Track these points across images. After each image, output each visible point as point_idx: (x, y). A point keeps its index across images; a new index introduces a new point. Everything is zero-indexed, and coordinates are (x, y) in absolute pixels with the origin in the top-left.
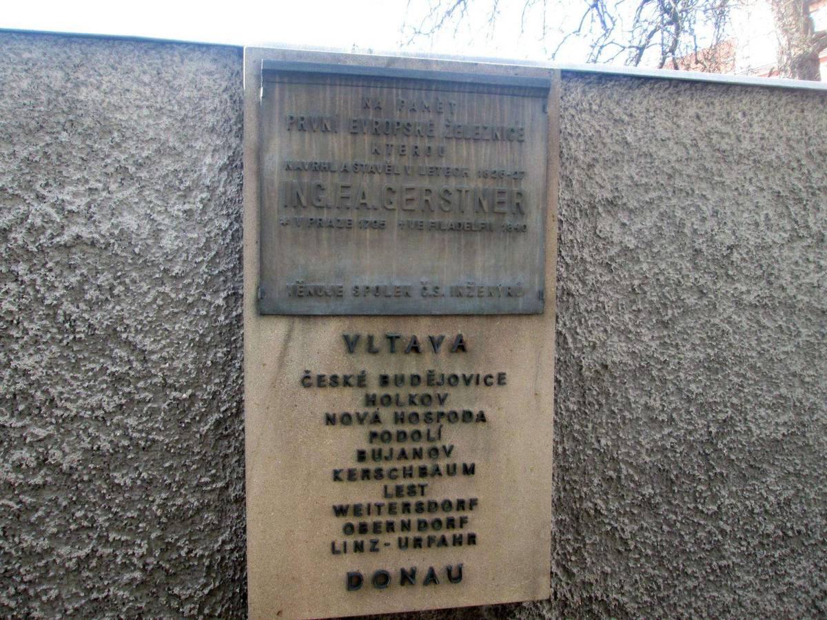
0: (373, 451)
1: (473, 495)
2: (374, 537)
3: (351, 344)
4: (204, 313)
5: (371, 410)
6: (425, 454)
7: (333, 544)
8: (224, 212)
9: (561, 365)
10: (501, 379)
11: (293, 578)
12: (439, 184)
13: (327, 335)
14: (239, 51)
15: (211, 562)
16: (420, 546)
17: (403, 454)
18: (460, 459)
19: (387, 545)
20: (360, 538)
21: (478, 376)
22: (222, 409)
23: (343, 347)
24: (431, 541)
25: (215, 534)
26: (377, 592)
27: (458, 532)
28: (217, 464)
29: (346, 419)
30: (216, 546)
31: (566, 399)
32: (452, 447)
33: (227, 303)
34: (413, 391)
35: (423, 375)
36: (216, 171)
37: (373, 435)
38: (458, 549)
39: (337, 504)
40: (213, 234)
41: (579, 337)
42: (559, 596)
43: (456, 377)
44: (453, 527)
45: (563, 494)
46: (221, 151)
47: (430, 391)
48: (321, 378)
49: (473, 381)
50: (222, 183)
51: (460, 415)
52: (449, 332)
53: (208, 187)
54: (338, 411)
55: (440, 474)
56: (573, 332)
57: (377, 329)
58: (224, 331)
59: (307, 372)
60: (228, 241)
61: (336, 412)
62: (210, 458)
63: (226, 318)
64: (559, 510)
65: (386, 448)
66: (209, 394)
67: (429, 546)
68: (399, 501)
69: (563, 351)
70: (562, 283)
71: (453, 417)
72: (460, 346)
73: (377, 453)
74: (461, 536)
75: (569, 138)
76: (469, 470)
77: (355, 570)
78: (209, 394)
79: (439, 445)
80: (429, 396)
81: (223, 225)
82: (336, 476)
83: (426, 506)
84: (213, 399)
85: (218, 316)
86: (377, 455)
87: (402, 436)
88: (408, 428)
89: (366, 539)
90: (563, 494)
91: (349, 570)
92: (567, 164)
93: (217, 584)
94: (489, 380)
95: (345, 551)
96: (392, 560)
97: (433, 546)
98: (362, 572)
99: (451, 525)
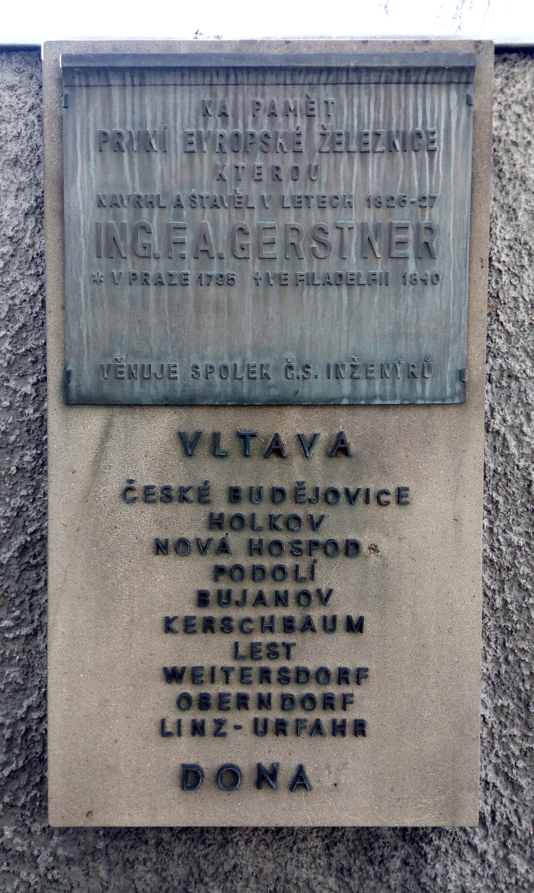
0: (220, 592)
1: (362, 664)
2: (220, 715)
3: (188, 444)
4: (7, 403)
5: (217, 536)
6: (291, 600)
7: (163, 722)
8: (32, 272)
9: (495, 479)
10: (401, 496)
11: (109, 767)
12: (313, 217)
13: (158, 429)
14: (32, 51)
15: (13, 733)
16: (285, 733)
17: (260, 599)
18: (342, 608)
19: (238, 727)
20: (200, 716)
21: (368, 490)
22: (30, 530)
23: (176, 451)
24: (299, 725)
25: (19, 696)
26: (223, 795)
27: (339, 715)
28: (22, 602)
29: (182, 546)
30: (20, 713)
31: (508, 528)
32: (330, 592)
33: (37, 390)
34: (276, 511)
35: (288, 489)
36: (21, 216)
37: (219, 571)
38: (339, 742)
39: (169, 665)
40: (17, 301)
41: (527, 439)
42: (498, 818)
43: (335, 492)
44: (332, 707)
45: (504, 667)
46: (27, 190)
47: (300, 511)
48: (148, 490)
49: (360, 499)
50: (28, 235)
51: (341, 546)
52: (322, 426)
53: (11, 238)
54: (171, 535)
55: (313, 630)
56: (517, 431)
57: (226, 424)
58: (33, 427)
59: (131, 481)
60: (37, 309)
61: (168, 536)
62: (13, 595)
63: (36, 411)
64: (499, 692)
65: (236, 589)
66: (13, 509)
67: (297, 733)
68: (255, 666)
69: (501, 459)
70: (500, 361)
71: (331, 548)
72: (340, 448)
73: (224, 595)
74: (344, 721)
75: (513, 148)
76: (355, 626)
77: (192, 761)
78: (13, 509)
79: (311, 588)
80: (297, 518)
81: (31, 288)
82: (168, 626)
83: (292, 675)
84: (18, 516)
85: (24, 408)
86: (224, 599)
87: (258, 573)
88: (267, 562)
89: (209, 717)
90: (504, 667)
91: (185, 761)
92: (509, 187)
93: (21, 763)
94: (384, 498)
95: (179, 734)
96: (244, 750)
97: (304, 734)
98: (203, 765)
99: (326, 706)
